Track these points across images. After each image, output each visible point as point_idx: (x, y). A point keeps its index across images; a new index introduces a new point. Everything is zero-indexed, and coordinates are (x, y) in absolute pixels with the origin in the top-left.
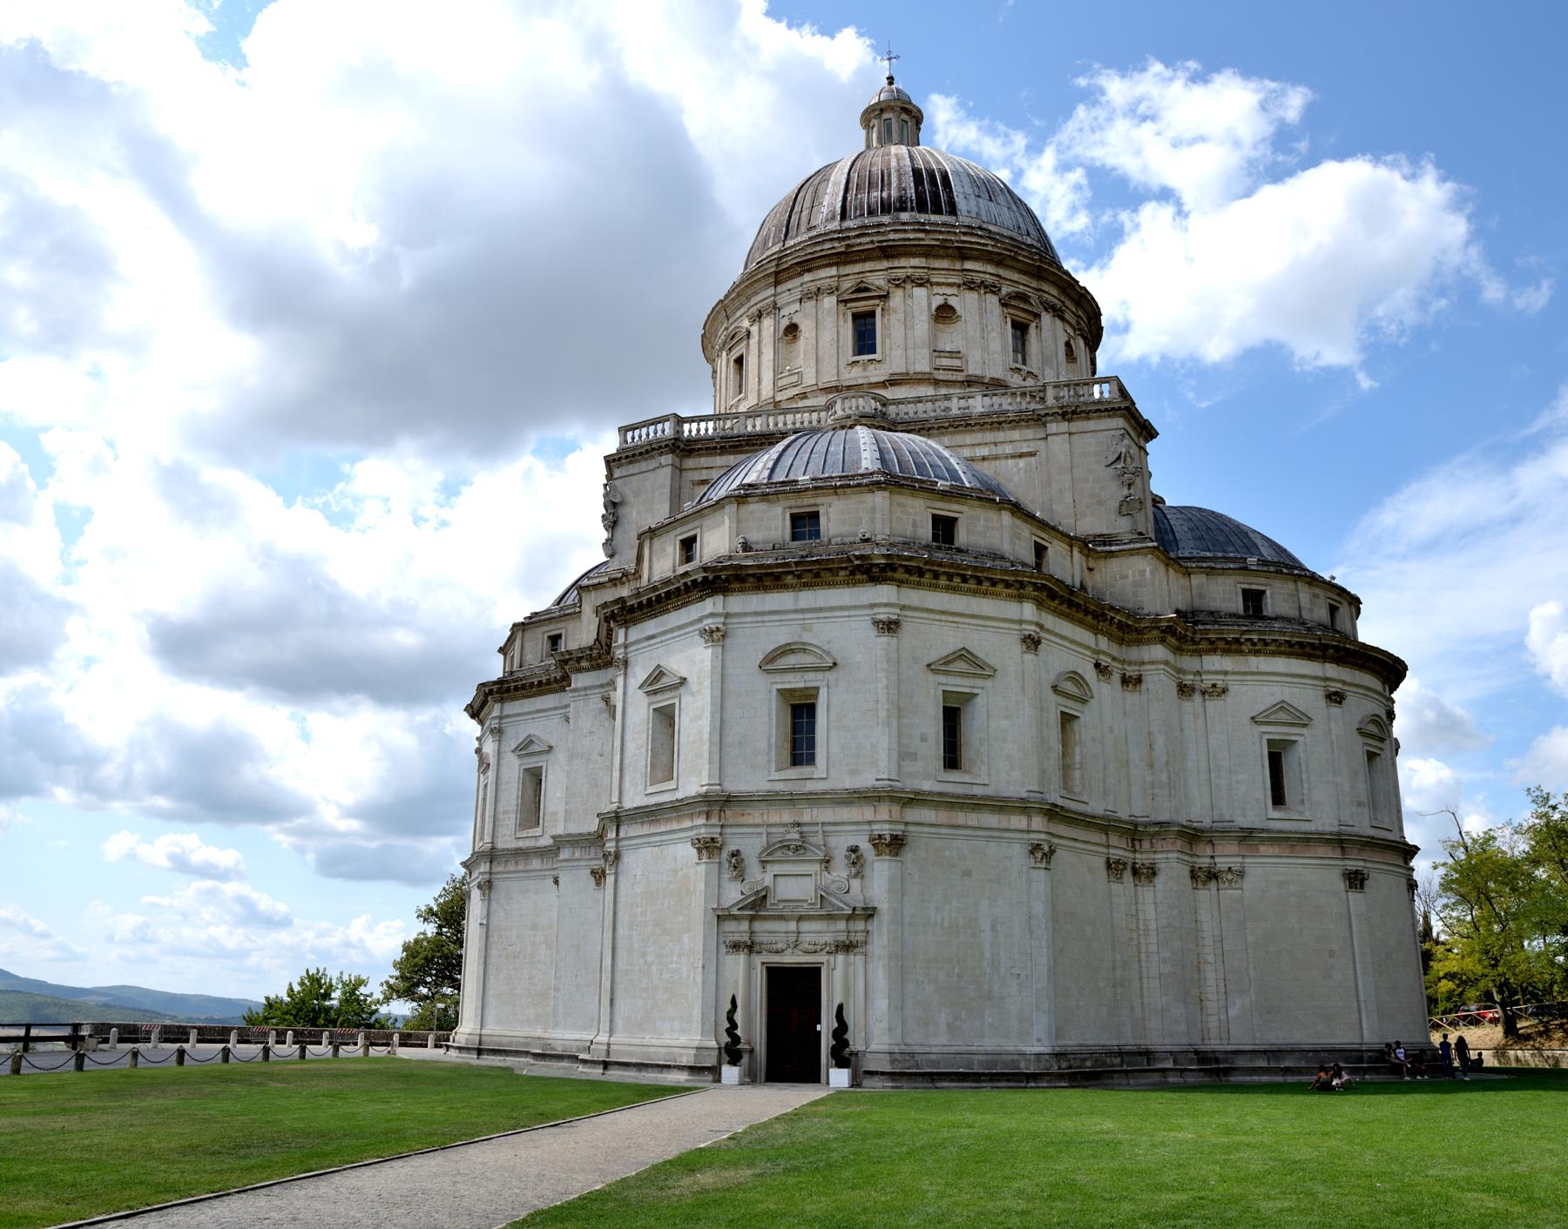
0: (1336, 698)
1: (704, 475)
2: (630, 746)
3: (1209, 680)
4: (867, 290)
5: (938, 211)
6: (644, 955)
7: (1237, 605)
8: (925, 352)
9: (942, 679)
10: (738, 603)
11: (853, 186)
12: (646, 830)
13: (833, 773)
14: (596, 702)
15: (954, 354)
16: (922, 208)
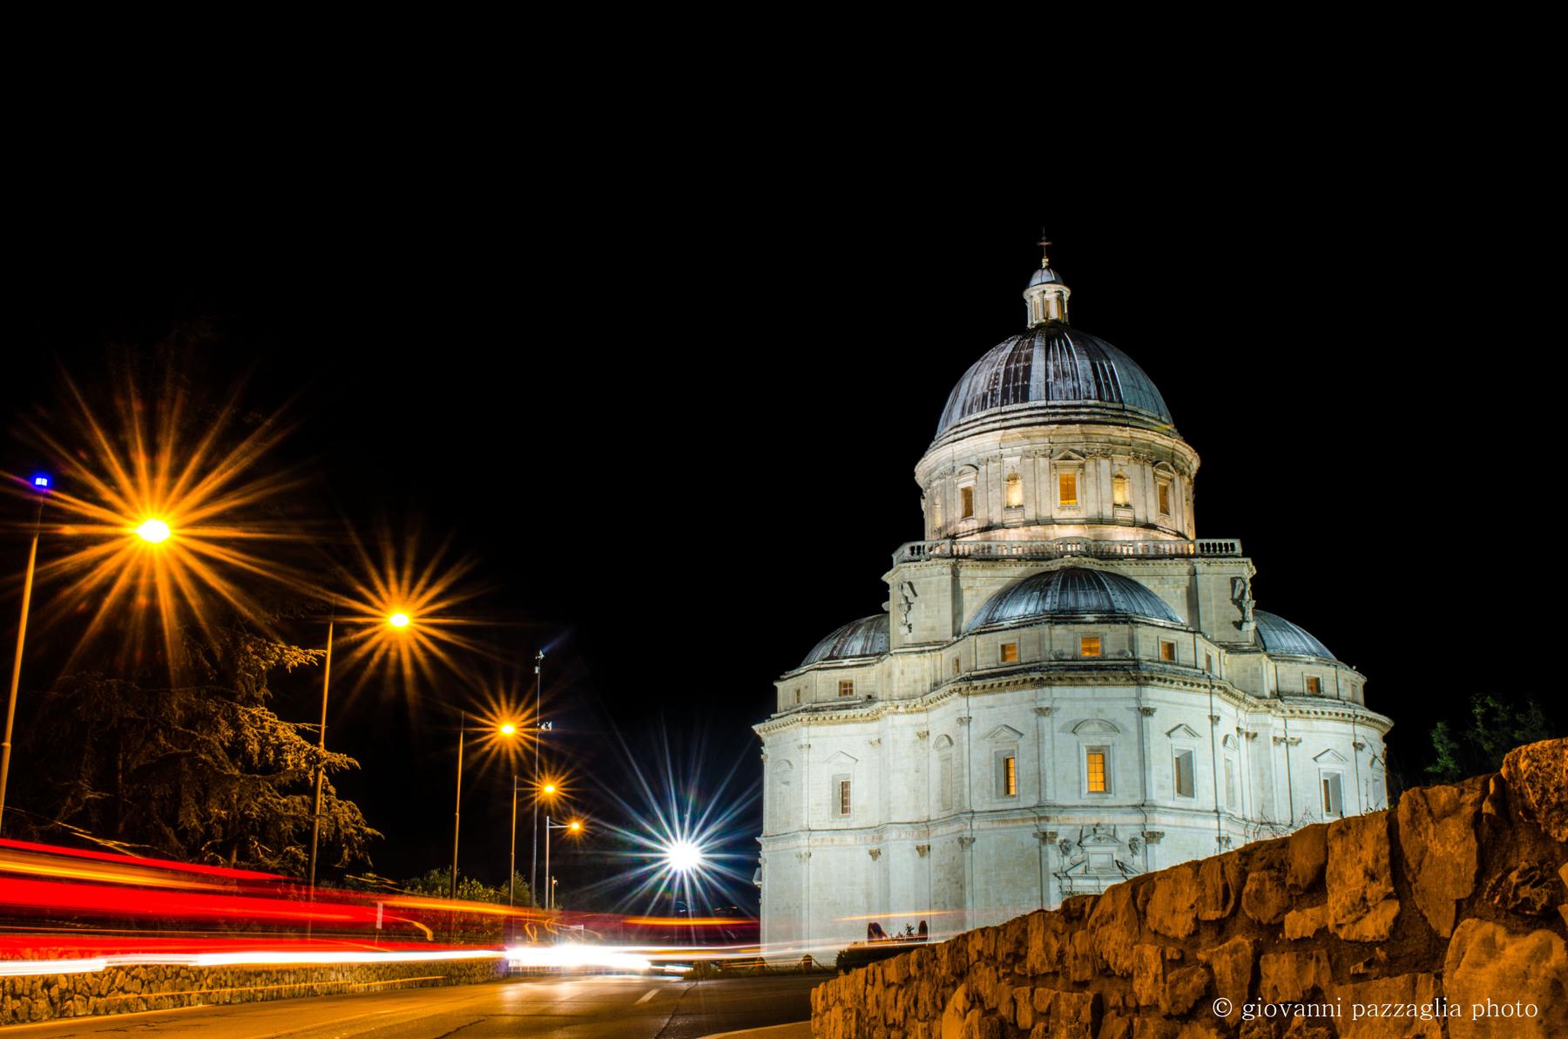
0: (1358, 746)
1: (971, 583)
2: (976, 773)
3: (1290, 735)
4: (1069, 458)
5: (1111, 400)
6: (999, 900)
7: (1302, 687)
8: (1110, 506)
9: (1172, 741)
10: (1057, 691)
11: (1051, 374)
12: (995, 825)
13: (1119, 795)
14: (910, 735)
15: (1127, 506)
16: (1100, 399)
